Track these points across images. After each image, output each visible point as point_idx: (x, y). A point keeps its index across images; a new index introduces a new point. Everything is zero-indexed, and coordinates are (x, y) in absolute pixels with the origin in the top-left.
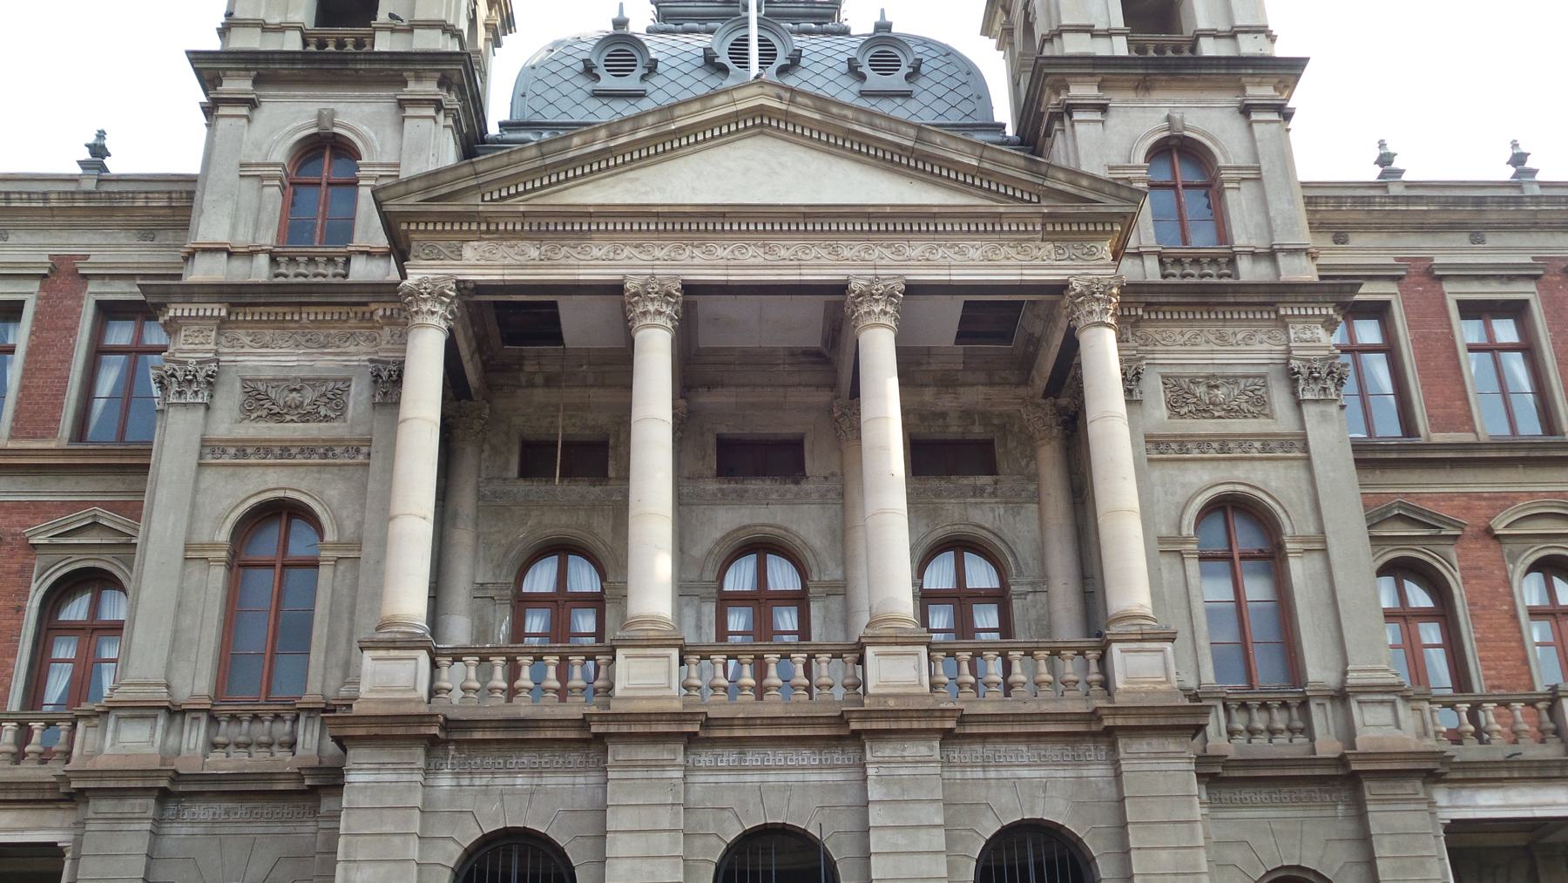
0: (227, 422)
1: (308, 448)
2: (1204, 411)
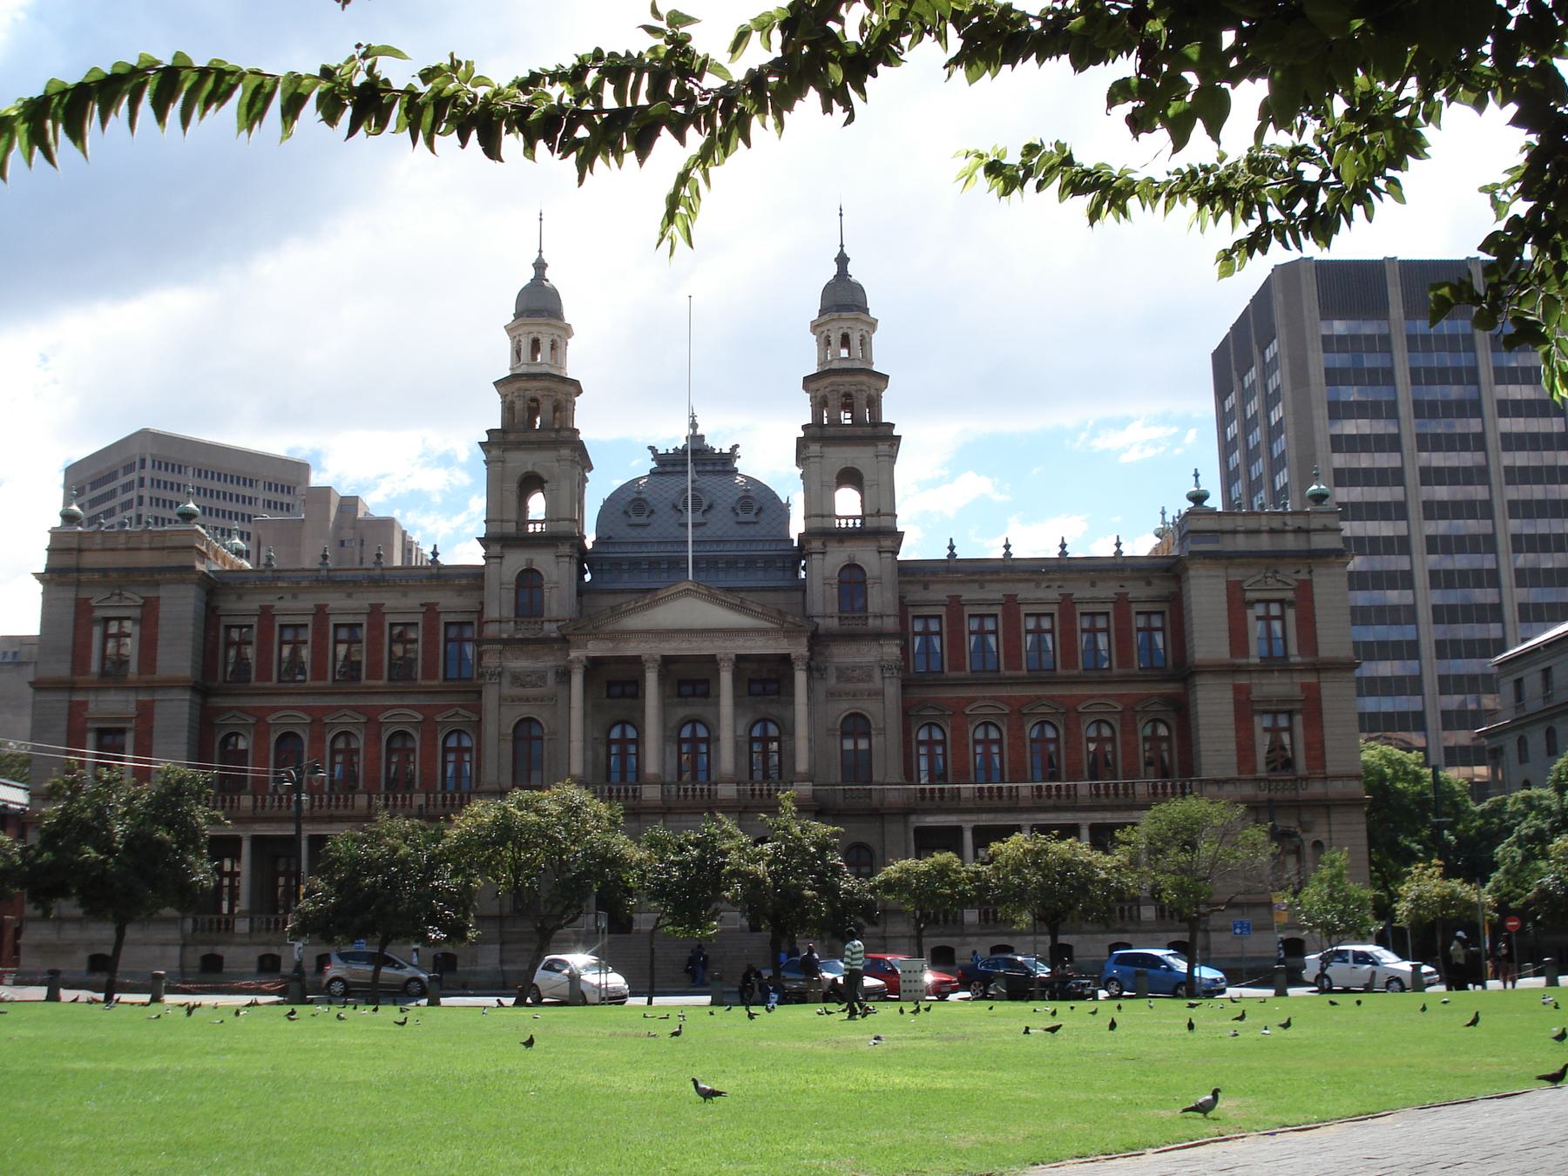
0: (508, 690)
1: (535, 699)
2: (849, 680)
